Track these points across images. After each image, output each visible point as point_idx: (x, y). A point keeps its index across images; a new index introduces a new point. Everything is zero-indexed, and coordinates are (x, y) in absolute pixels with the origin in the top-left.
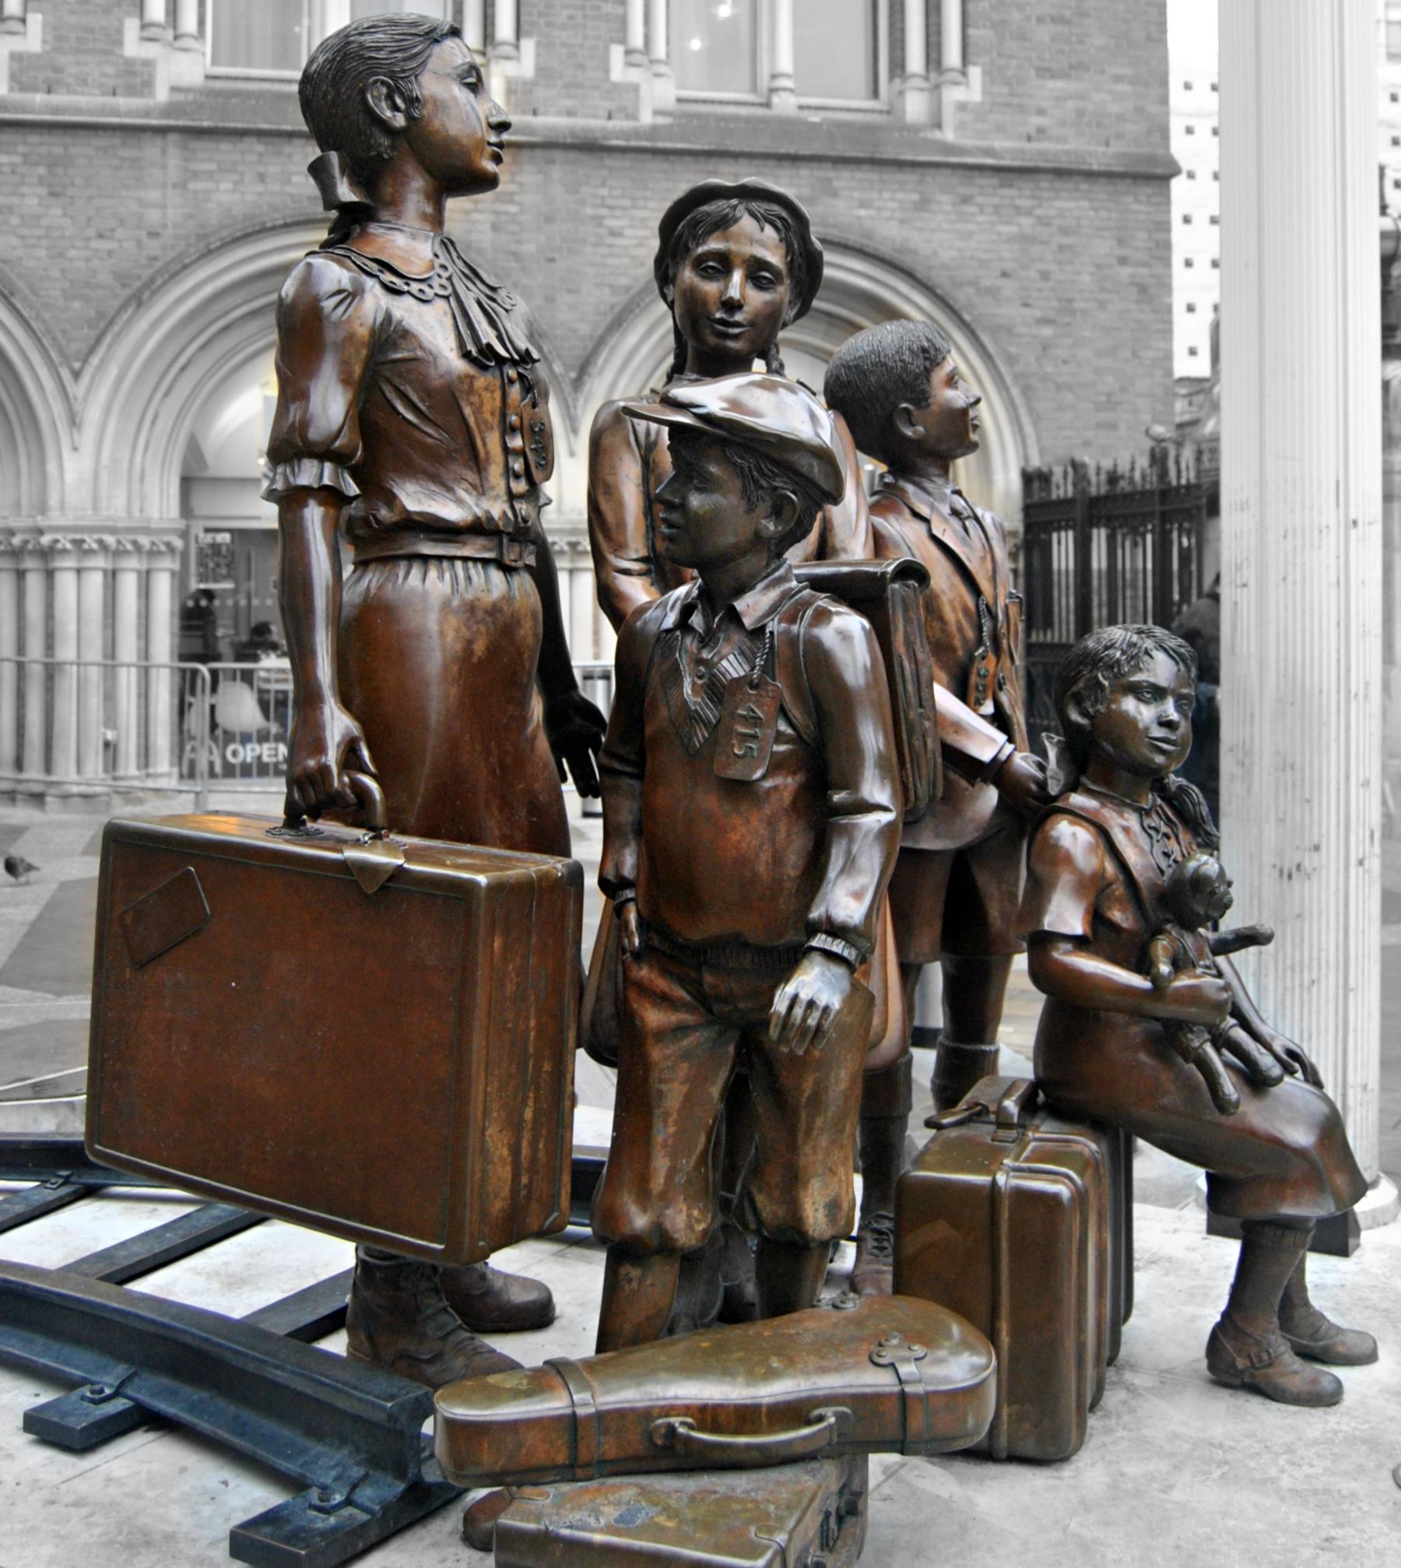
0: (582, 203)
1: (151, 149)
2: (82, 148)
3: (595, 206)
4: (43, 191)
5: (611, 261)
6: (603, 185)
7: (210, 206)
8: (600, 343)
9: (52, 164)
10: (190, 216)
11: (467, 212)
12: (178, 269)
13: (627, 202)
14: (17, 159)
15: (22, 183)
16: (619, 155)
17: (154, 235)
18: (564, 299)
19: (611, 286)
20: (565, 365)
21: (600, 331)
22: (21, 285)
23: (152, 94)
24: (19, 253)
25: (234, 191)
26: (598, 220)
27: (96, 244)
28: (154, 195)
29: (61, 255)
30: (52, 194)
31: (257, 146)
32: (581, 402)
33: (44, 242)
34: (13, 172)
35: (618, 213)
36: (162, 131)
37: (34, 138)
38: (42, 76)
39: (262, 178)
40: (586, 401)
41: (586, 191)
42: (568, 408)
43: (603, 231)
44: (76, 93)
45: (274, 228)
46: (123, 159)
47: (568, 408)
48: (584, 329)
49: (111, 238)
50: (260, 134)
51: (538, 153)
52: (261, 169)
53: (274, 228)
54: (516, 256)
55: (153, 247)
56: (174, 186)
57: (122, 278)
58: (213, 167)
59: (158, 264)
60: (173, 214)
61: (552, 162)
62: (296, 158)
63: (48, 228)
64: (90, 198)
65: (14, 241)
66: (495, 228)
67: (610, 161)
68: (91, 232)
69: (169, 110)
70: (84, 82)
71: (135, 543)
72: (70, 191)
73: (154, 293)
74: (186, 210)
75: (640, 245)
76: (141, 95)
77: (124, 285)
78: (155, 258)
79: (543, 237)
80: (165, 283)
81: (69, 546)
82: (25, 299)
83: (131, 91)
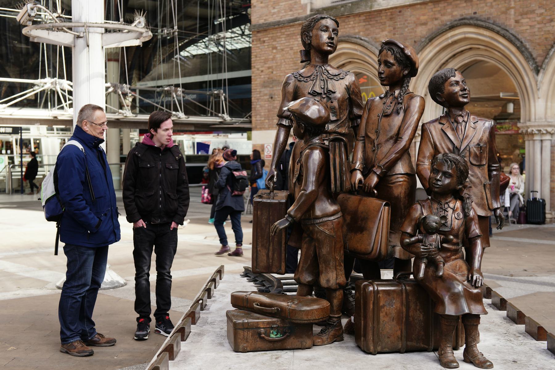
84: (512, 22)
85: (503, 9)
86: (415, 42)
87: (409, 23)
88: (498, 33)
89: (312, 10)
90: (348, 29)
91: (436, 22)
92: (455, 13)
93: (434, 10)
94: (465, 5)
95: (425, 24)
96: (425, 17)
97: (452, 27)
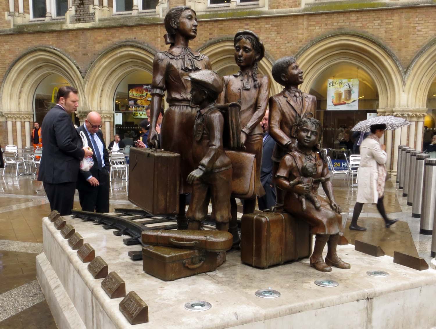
0: (410, 23)
1: (300, 20)
2: (285, 21)
3: (414, 24)
4: (276, 33)
5: (418, 38)
6: (417, 18)
7: (314, 33)
8: (413, 61)
9: (278, 26)
10: (309, 36)
11: (378, 28)
12: (306, 49)
13: (423, 22)
14: (270, 26)
15: (271, 31)
16: (422, 9)
17: (301, 41)
18: (404, 50)
19: (417, 46)
20: (403, 68)
21: (413, 58)
22: (271, 56)
23: (300, 6)
24: (270, 48)
25: (319, 29)
26: (414, 28)
27: (287, 45)
28: (300, 32)
29: (280, 48)
30: (278, 33)
31: (325, 17)
32: (406, 77)
33: (276, 45)
34: (269, 29)
35: (420, 25)
36: (303, 15)
37: (274, 20)
38: (275, 5)
39: (326, 25)
40: (408, 77)
41: (411, 20)
42: (403, 79)
43: (416, 30)
44: (283, 8)
45: (329, 37)
46: (294, 23)
47: (403, 79)
48: (409, 57)
49: (291, 43)
50: (326, 13)
51: (399, 10)
52: (326, 22)
53: (329, 37)
54: (391, 39)
55: (300, 44)
56: (305, 29)
57: (293, 52)
58: (315, 23)
59: (301, 48)
60: (305, 36)
61: (403, 13)
62: (335, 19)
63: (277, 42)
64: (286, 34)
65: (269, 45)
66: (386, 32)
67: (419, 11)
68: (286, 42)
69: (305, 10)
70: (285, 5)
71: (416, 114)
72: (282, 32)
73: (300, 56)
74: (308, 35)
75: (426, 33)
76: (298, 7)
77: (294, 54)
78: (301, 47)
79: (399, 34)
80: (302, 53)
81: (400, 115)
82: (271, 59)
83: (296, 6)
84: (159, 46)
85: (153, 37)
86: (94, 54)
87: (89, 41)
88: (150, 53)
89: (14, 25)
90: (44, 42)
91: (109, 42)
92: (122, 37)
93: (107, 33)
94: (128, 32)
95: (100, 42)
96: (101, 38)
97: (120, 46)
